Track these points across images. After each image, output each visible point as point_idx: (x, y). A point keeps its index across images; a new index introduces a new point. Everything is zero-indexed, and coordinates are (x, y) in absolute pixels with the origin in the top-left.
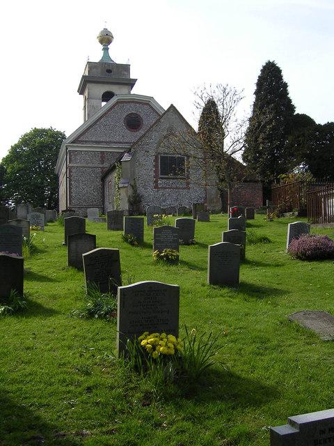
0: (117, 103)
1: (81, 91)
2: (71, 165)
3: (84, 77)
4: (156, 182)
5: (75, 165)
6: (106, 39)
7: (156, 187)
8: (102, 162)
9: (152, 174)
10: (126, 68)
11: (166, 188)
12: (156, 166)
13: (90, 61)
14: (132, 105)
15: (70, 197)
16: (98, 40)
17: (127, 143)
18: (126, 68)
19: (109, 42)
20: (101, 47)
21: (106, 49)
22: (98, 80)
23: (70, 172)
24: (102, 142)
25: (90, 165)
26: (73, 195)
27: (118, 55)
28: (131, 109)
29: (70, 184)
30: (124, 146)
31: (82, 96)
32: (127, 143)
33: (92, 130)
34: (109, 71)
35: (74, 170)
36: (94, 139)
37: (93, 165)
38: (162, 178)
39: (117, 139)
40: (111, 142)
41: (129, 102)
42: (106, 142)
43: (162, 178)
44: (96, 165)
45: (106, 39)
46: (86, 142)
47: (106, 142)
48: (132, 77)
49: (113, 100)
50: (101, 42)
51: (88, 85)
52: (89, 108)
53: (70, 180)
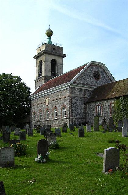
2: (72, 95)
5: (74, 95)
6: (50, 34)
8: (85, 95)
10: (61, 49)
15: (72, 112)
16: (45, 34)
17: (94, 86)
18: (61, 49)
19: (51, 35)
20: (47, 37)
21: (50, 39)
23: (72, 99)
26: (73, 111)
27: (56, 41)
28: (96, 69)
29: (72, 105)
32: (94, 86)
34: (54, 49)
35: (73, 98)
39: (90, 83)
42: (86, 85)
44: (83, 96)
45: (50, 34)
46: (78, 83)
47: (86, 85)
48: (64, 53)
50: (47, 35)
53: (72, 103)
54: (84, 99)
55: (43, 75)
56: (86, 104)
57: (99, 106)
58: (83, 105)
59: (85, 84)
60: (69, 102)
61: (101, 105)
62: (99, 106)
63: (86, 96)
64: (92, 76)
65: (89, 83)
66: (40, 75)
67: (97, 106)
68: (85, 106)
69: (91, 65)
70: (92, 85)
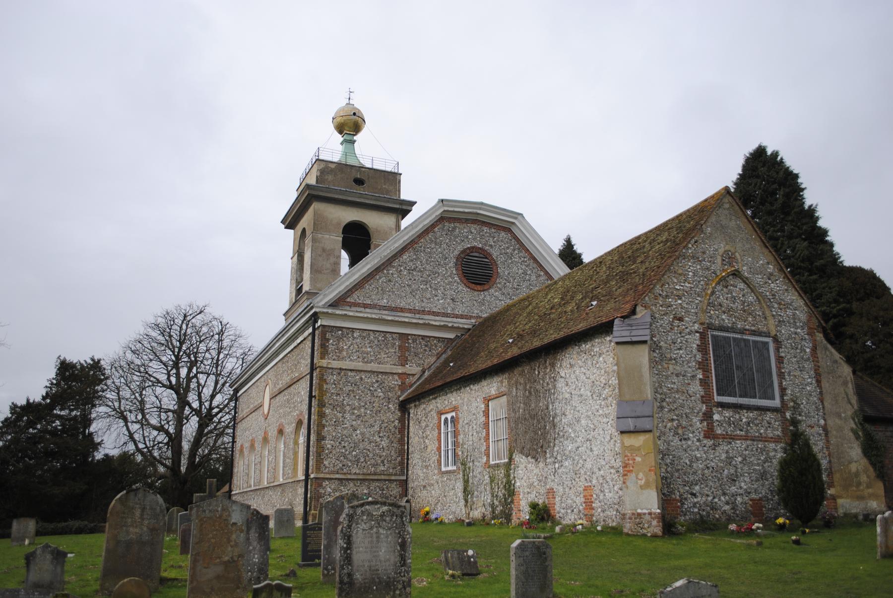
1: (291, 222)
2: (324, 363)
4: (708, 416)
5: (336, 364)
7: (709, 433)
8: (403, 361)
9: (696, 388)
11: (733, 438)
12: (703, 366)
13: (321, 157)
14: (474, 228)
18: (392, 178)
20: (339, 138)
22: (336, 196)
24: (402, 310)
26: (328, 443)
28: (472, 238)
29: (321, 415)
30: (450, 322)
31: (291, 232)
32: (462, 317)
33: (382, 279)
34: (359, 182)
35: (331, 378)
36: (384, 302)
38: (723, 405)
39: (438, 304)
40: (423, 312)
41: (467, 221)
43: (723, 405)
44: (387, 368)
48: (403, 196)
50: (340, 128)
53: (322, 405)
54: (395, 382)
55: (306, 288)
56: (404, 407)
57: (449, 416)
58: (392, 414)
59: (410, 311)
60: (311, 397)
61: (455, 409)
62: (449, 416)
63: (412, 368)
64: (450, 271)
65: (428, 306)
66: (299, 291)
67: (440, 413)
68: (402, 420)
69: (442, 219)
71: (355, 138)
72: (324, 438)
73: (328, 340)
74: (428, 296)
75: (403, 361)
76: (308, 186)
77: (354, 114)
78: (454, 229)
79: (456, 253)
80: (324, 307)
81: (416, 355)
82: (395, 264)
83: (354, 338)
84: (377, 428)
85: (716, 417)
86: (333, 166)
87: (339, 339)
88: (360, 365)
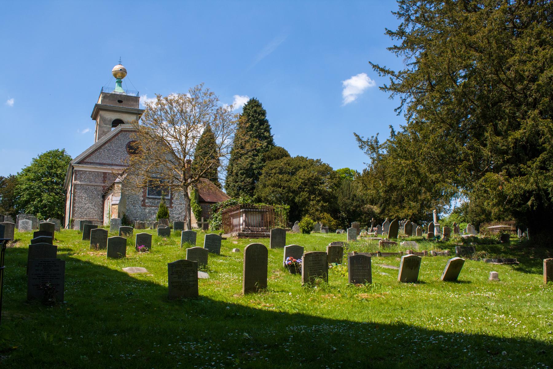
0: (121, 131)
1: (94, 117)
3: (97, 105)
8: (104, 181)
11: (152, 206)
14: (133, 134)
15: (73, 210)
25: (93, 184)
26: (76, 209)
31: (95, 121)
33: (97, 153)
36: (98, 161)
37: (96, 184)
38: (149, 198)
39: (119, 161)
41: (131, 131)
43: (149, 198)
44: (98, 184)
47: (109, 165)
49: (120, 127)
51: (101, 113)
52: (102, 133)
54: (101, 188)
58: (100, 199)
65: (114, 162)
70: (121, 166)
71: (122, 80)
72: (75, 207)
73: (77, 175)
74: (115, 159)
75: (104, 181)
76: (97, 105)
77: (121, 70)
78: (126, 134)
79: (126, 143)
80: (75, 163)
81: (109, 179)
82: (103, 148)
83: (87, 174)
84: (94, 204)
85: (146, 201)
86: (109, 95)
87: (81, 174)
88: (88, 183)
